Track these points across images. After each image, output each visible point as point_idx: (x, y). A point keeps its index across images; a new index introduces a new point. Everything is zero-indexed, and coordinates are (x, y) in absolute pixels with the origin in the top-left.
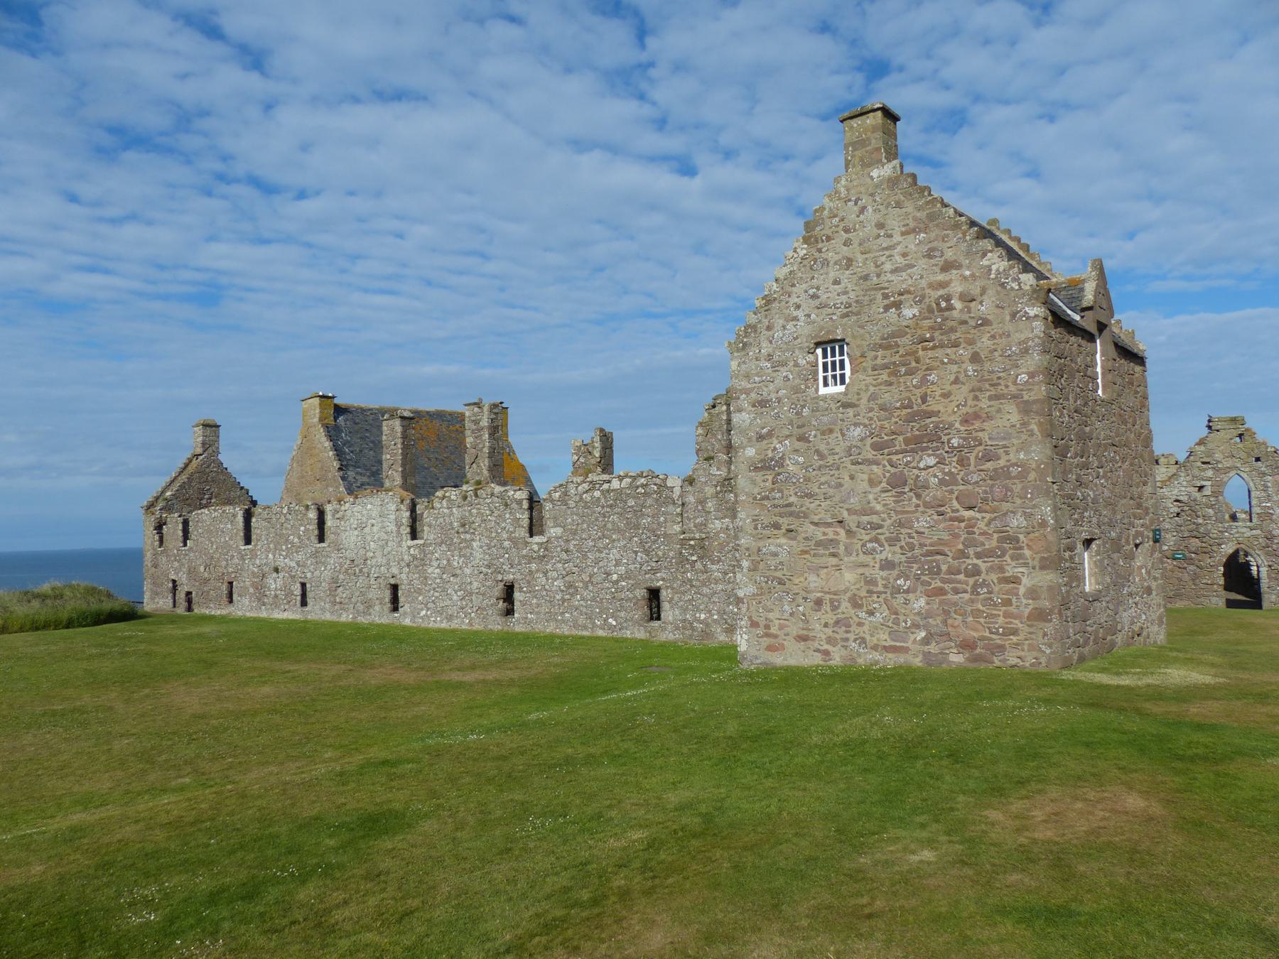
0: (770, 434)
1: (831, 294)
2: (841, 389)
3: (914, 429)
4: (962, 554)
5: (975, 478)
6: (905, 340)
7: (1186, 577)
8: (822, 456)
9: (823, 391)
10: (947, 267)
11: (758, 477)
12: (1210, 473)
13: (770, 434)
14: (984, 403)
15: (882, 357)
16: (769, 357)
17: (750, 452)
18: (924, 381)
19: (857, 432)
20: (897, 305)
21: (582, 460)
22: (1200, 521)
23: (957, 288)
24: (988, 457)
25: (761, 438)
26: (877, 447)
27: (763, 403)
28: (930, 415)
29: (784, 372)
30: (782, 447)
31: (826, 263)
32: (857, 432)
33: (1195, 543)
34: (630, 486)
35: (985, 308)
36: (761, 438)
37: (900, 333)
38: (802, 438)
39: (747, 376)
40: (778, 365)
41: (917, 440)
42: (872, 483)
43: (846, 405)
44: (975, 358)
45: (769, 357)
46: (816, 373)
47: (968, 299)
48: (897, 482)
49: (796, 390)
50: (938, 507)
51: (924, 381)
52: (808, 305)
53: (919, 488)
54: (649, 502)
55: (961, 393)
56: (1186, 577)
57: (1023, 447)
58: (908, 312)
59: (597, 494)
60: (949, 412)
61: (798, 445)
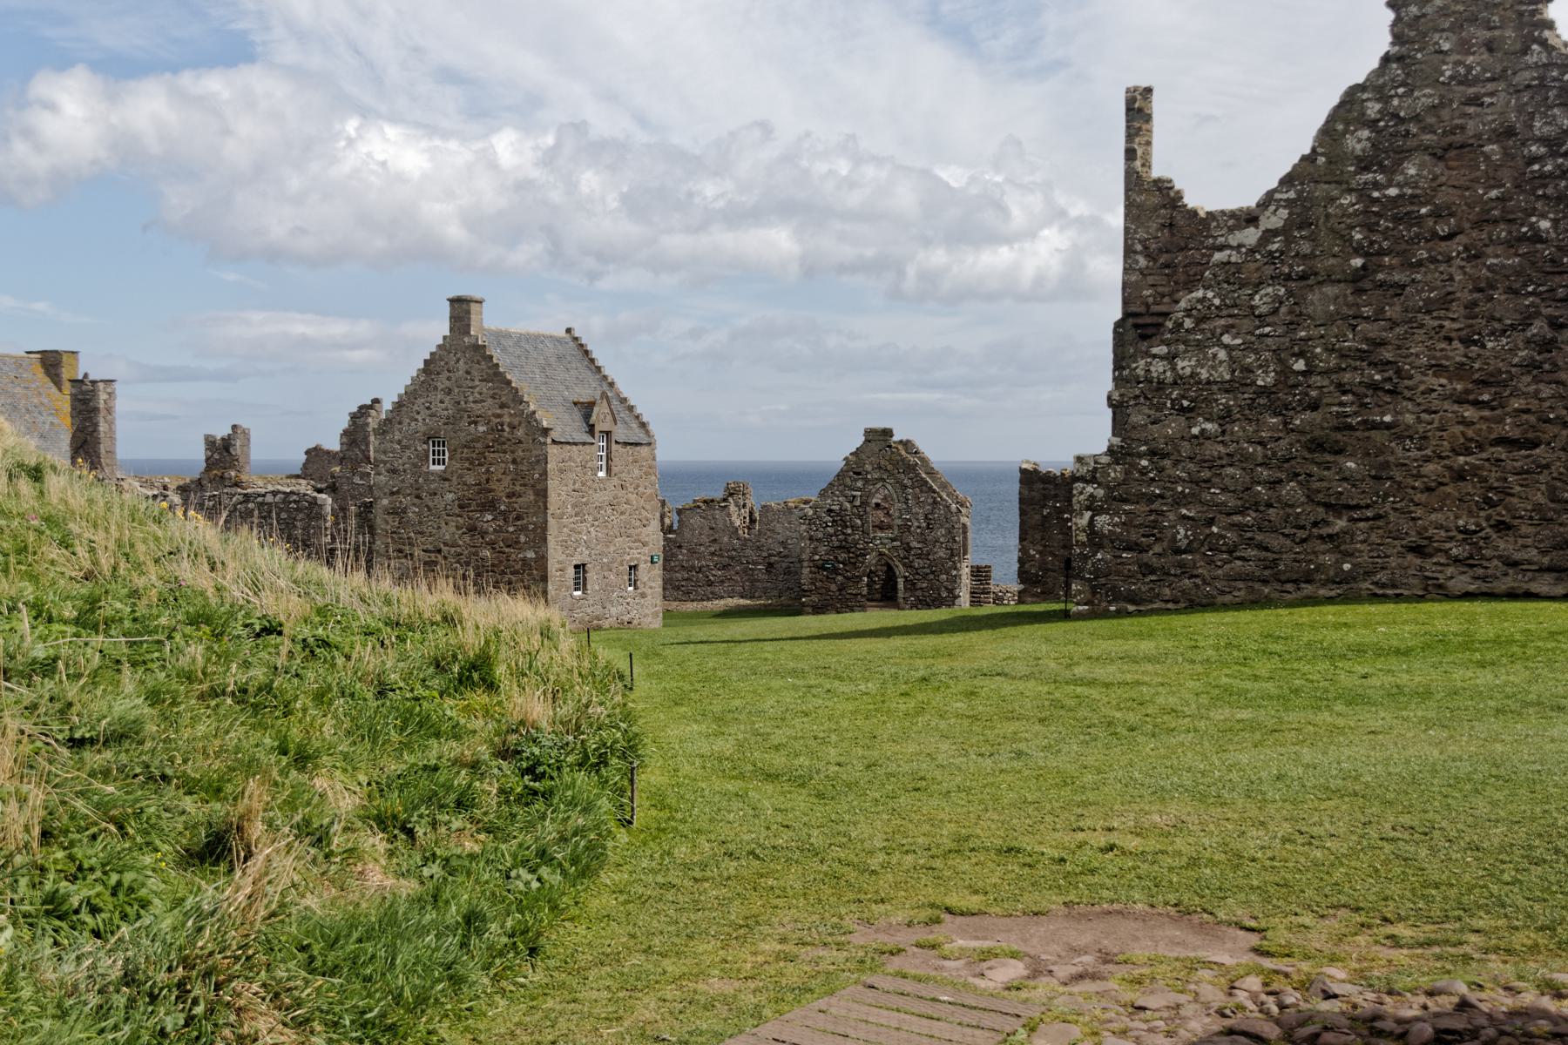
0: (398, 492)
1: (438, 408)
2: (442, 467)
3: (482, 499)
4: (503, 573)
5: (511, 529)
6: (478, 445)
7: (833, 587)
8: (430, 509)
9: (432, 467)
10: (502, 406)
11: (389, 518)
12: (860, 484)
13: (398, 492)
14: (518, 488)
15: (466, 453)
16: (399, 442)
17: (385, 502)
18: (488, 471)
19: (450, 496)
20: (476, 423)
21: (216, 456)
22: (849, 531)
23: (507, 419)
24: (518, 518)
25: (392, 493)
26: (461, 507)
27: (394, 471)
28: (491, 491)
29: (408, 453)
30: (406, 501)
31: (436, 388)
32: (450, 496)
33: (843, 556)
34: (284, 502)
35: (520, 433)
36: (392, 493)
37: (477, 440)
38: (418, 497)
39: (385, 452)
40: (404, 448)
41: (483, 505)
42: (458, 528)
43: (446, 479)
44: (514, 462)
45: (399, 442)
46: (427, 457)
47: (513, 427)
48: (472, 529)
49: (415, 465)
50: (492, 544)
51: (488, 471)
52: (425, 413)
53: (483, 534)
54: (301, 516)
55: (507, 480)
56: (833, 587)
57: (535, 514)
58: (481, 429)
59: (251, 505)
60: (500, 489)
61: (416, 501)
